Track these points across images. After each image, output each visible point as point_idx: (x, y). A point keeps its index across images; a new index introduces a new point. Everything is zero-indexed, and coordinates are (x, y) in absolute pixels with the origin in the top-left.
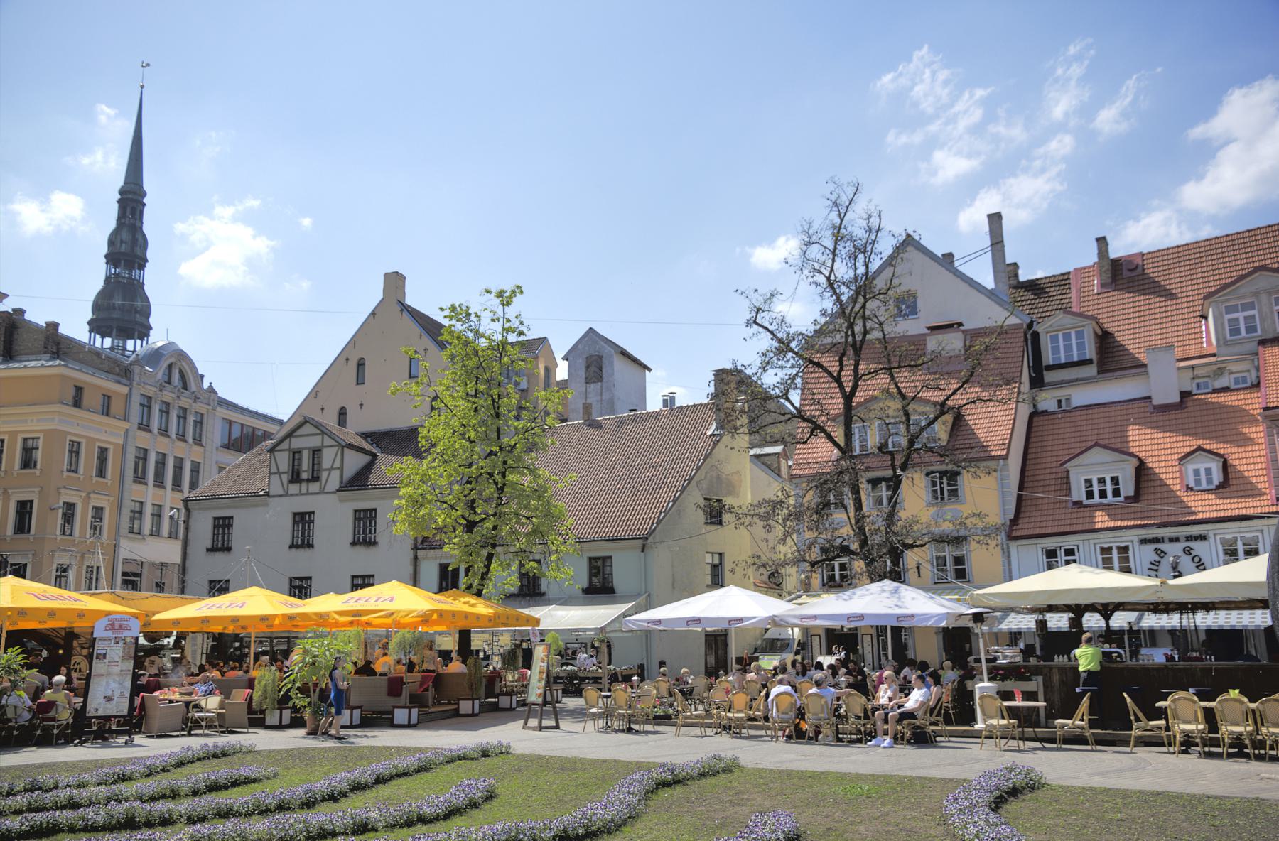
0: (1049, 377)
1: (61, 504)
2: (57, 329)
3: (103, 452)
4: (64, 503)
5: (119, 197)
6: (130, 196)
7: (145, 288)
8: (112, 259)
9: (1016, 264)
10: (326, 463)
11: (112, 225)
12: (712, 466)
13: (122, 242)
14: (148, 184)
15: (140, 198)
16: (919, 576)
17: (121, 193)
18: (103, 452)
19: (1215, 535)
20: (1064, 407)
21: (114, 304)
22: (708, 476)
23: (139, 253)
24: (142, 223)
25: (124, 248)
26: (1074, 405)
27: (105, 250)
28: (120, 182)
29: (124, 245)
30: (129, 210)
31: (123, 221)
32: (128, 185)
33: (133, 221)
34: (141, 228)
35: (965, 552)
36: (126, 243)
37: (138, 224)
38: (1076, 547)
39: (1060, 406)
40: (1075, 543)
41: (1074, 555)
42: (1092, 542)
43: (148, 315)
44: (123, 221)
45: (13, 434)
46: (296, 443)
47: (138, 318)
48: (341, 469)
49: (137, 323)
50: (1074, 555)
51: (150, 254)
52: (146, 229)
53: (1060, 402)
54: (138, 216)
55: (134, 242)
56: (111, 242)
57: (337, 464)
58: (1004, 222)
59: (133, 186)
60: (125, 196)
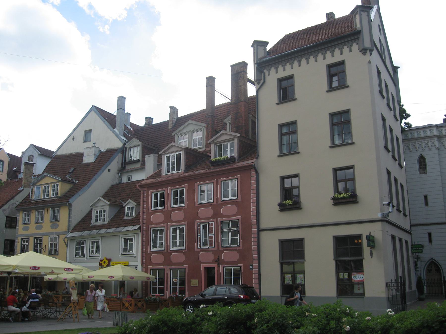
0: (128, 167)
9: (149, 118)
12: (13, 203)
19: (121, 237)
20: (130, 181)
22: (11, 207)
26: (132, 180)
35: (57, 242)
38: (85, 241)
39: (129, 180)
40: (85, 239)
41: (84, 245)
42: (89, 239)
50: (84, 245)
53: (129, 178)
58: (126, 99)
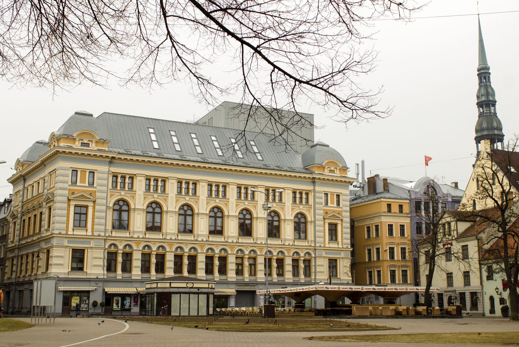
1: (388, 249)
2: (387, 181)
3: (402, 227)
4: (390, 248)
5: (478, 73)
6: (482, 71)
7: (498, 115)
8: (480, 105)
10: (452, 228)
11: (478, 87)
13: (482, 95)
14: (490, 63)
15: (487, 71)
17: (478, 70)
18: (402, 227)
21: (483, 128)
23: (491, 99)
24: (490, 83)
25: (483, 99)
27: (476, 101)
28: (475, 65)
29: (483, 97)
30: (483, 78)
31: (481, 84)
32: (480, 66)
33: (485, 84)
34: (490, 86)
36: (484, 95)
37: (488, 84)
43: (501, 129)
44: (481, 84)
45: (372, 224)
46: (443, 221)
47: (496, 132)
48: (457, 230)
49: (495, 135)
51: (497, 98)
52: (493, 85)
54: (487, 80)
55: (487, 94)
56: (478, 97)
57: (455, 229)
59: (482, 65)
60: (480, 72)
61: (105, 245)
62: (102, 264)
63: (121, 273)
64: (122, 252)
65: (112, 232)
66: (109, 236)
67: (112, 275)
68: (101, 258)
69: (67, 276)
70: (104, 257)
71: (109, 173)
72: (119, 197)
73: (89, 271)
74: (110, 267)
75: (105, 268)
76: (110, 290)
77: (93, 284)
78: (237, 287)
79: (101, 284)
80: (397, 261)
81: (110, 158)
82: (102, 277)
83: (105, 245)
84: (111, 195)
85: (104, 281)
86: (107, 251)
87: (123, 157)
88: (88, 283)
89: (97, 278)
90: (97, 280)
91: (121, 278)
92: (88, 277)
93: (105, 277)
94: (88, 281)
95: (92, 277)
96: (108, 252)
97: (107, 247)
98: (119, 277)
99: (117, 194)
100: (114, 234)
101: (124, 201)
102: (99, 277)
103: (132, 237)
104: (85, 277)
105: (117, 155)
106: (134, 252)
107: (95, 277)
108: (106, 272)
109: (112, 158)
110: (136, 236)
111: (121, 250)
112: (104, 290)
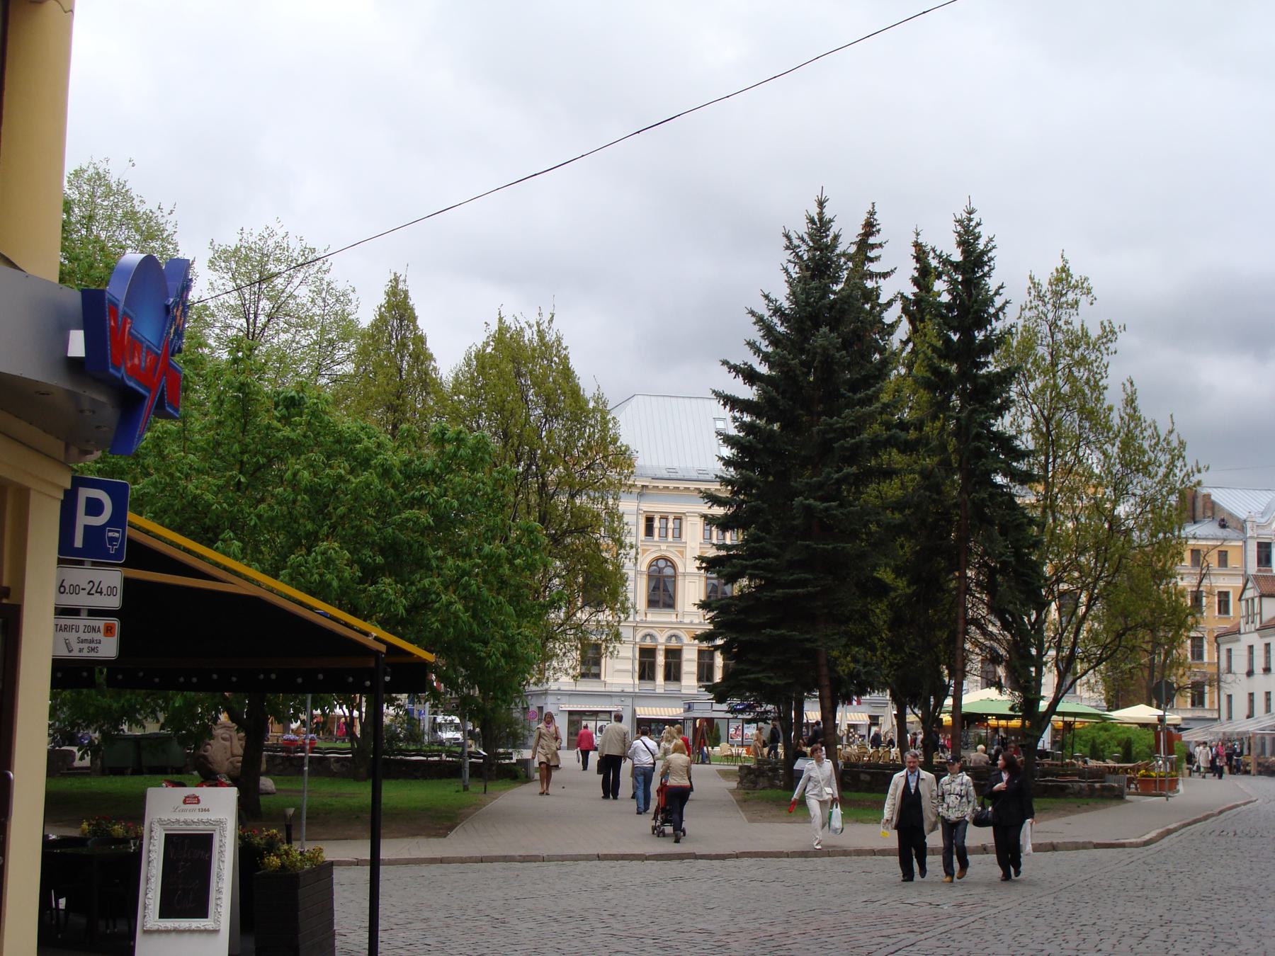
16: (1251, 695)
61: (634, 637)
62: (630, 667)
63: (663, 683)
64: (664, 647)
65: (646, 614)
66: (642, 621)
67: (647, 686)
68: (629, 658)
69: (573, 688)
70: (634, 656)
71: (638, 514)
72: (657, 554)
73: (608, 680)
74: (646, 672)
75: (637, 675)
76: (646, 712)
77: (616, 700)
78: (872, 709)
79: (629, 701)
80: (1209, 664)
81: (638, 488)
82: (631, 690)
83: (634, 637)
84: (644, 551)
85: (634, 696)
86: (638, 646)
87: (661, 484)
88: (607, 700)
89: (623, 691)
90: (622, 695)
91: (662, 691)
92: (607, 689)
93: (637, 690)
94: (608, 695)
95: (614, 689)
96: (640, 648)
97: (638, 640)
98: (660, 690)
99: (655, 549)
100: (650, 618)
101: (666, 559)
102: (626, 690)
103: (681, 623)
104: (603, 689)
105: (650, 482)
106: (684, 647)
107: (619, 689)
108: (637, 681)
109: (643, 486)
110: (687, 620)
111: (661, 644)
112: (634, 711)
